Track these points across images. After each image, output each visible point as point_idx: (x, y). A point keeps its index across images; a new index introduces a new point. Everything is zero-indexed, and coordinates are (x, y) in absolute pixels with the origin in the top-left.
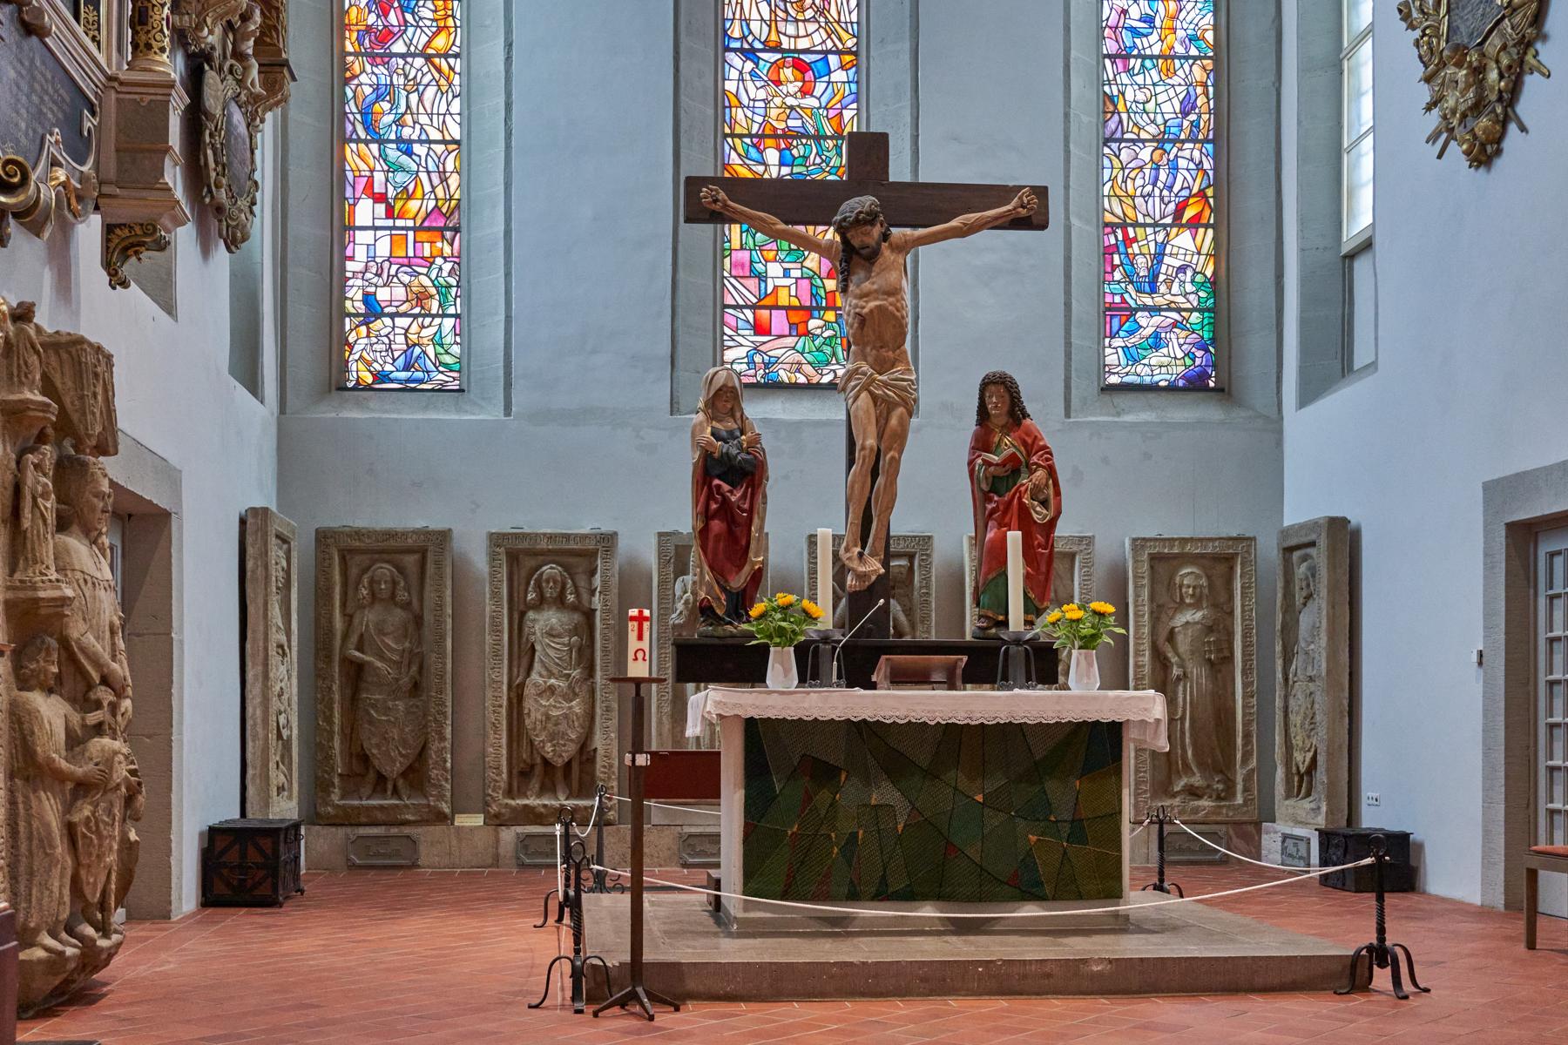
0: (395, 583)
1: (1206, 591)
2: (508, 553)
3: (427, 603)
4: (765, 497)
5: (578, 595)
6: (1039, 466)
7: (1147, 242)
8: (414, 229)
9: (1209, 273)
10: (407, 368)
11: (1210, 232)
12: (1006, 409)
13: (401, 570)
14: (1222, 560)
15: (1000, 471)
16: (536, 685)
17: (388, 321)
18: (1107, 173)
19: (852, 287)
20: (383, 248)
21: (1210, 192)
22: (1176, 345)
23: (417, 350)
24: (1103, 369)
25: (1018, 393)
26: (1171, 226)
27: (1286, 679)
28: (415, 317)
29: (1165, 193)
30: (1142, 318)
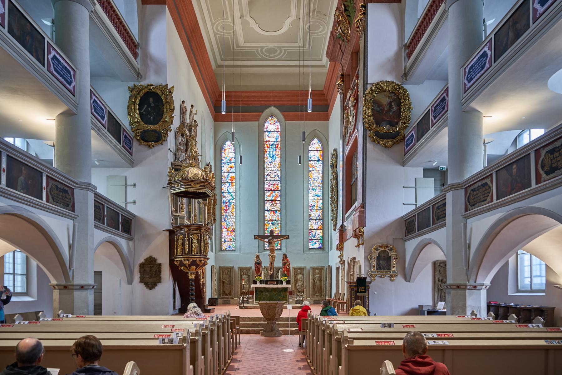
14: (321, 269)
20: (226, 234)
22: (318, 244)
24: (309, 246)
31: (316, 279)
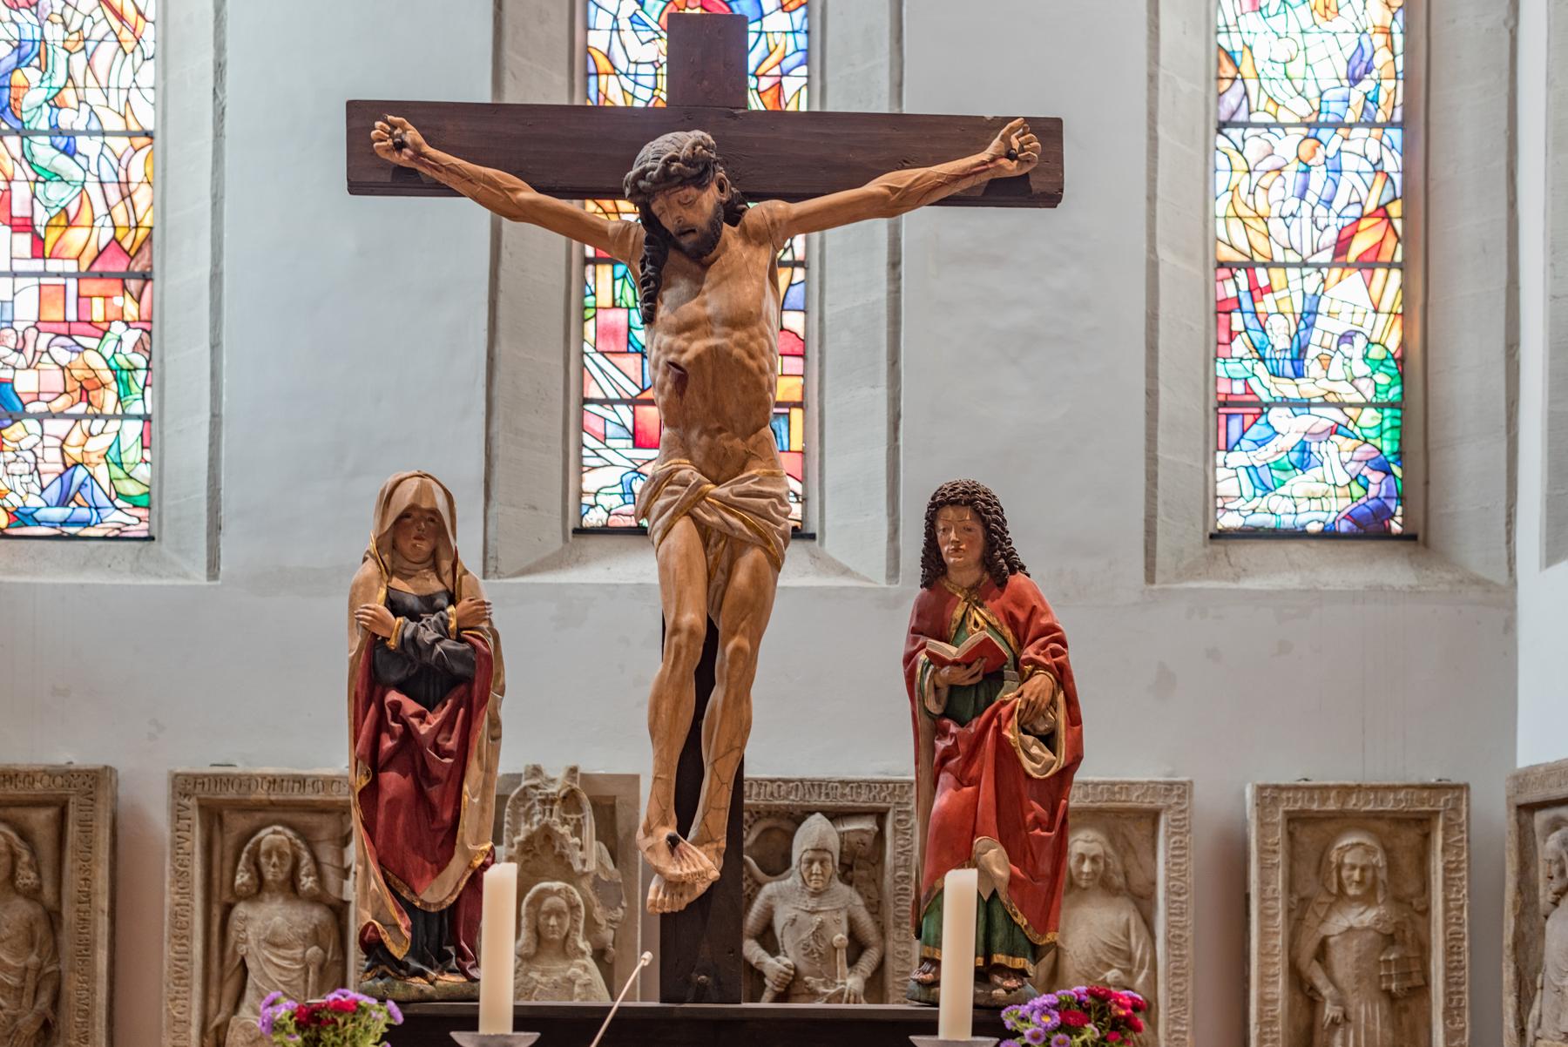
0: (14, 856)
1: (1383, 875)
2: (201, 807)
3: (66, 890)
4: (495, 724)
5: (320, 877)
6: (1038, 665)
7: (1290, 290)
8: (79, 277)
9: (1393, 343)
10: (63, 501)
11: (1396, 275)
12: (977, 552)
13: (25, 835)
14: (1411, 826)
15: (962, 677)
16: (246, 1028)
17: (32, 425)
18: (1222, 180)
19: (663, 312)
21: (1395, 210)
23: (80, 474)
24: (1209, 499)
25: (1002, 523)
26: (1329, 266)
27: (1522, 1032)
28: (77, 418)
29: (1321, 211)
30: (1277, 416)
31: (1344, 961)
